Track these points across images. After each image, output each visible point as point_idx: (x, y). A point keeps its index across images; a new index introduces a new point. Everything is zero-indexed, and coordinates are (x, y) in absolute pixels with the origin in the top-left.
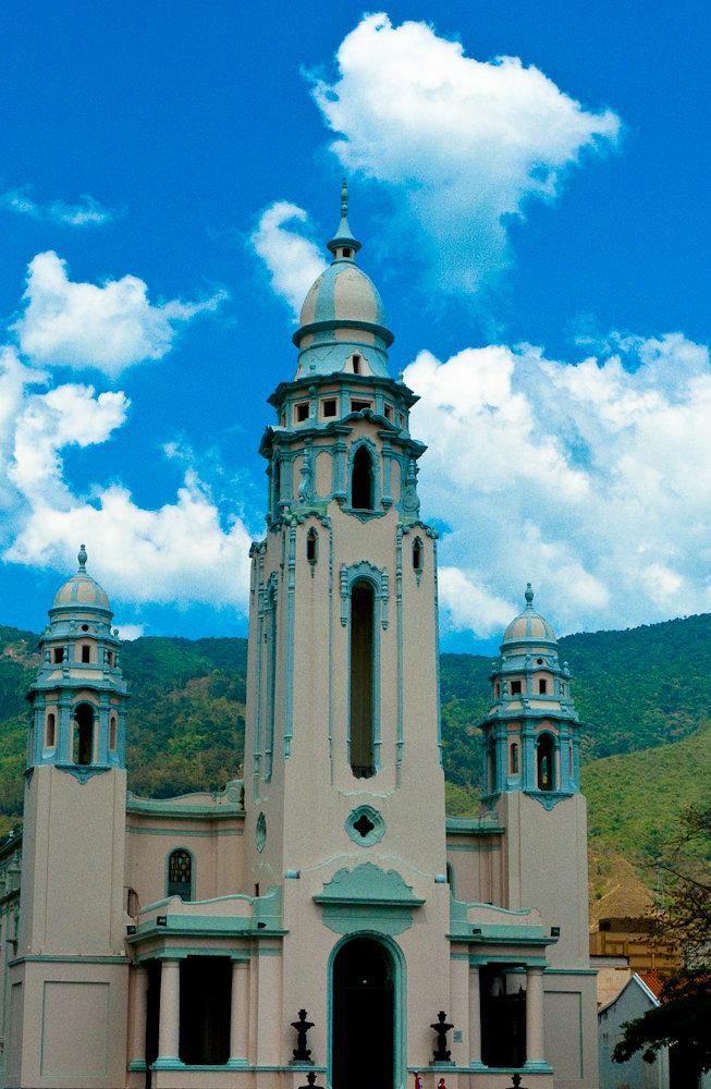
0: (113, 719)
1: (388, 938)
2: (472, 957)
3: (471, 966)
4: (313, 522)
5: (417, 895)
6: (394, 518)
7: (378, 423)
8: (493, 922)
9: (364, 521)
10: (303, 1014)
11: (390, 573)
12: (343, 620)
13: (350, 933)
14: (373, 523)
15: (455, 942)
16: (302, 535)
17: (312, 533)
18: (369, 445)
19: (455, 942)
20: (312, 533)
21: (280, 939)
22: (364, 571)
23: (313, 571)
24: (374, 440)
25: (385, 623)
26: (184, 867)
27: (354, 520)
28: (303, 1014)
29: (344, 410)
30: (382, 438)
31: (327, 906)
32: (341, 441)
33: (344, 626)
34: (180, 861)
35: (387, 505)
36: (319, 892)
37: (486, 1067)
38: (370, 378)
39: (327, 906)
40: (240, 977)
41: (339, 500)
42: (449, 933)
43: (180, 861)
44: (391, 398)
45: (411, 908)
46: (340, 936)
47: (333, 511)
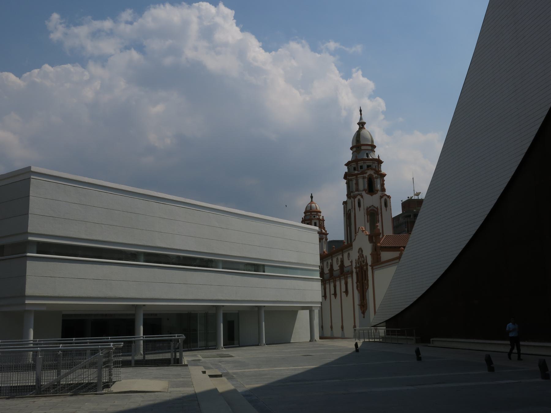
4: (359, 197)
7: (372, 169)
11: (379, 208)
14: (374, 196)
16: (356, 200)
17: (359, 200)
20: (359, 200)
25: (378, 221)
27: (369, 196)
29: (365, 167)
35: (378, 191)
47: (364, 193)
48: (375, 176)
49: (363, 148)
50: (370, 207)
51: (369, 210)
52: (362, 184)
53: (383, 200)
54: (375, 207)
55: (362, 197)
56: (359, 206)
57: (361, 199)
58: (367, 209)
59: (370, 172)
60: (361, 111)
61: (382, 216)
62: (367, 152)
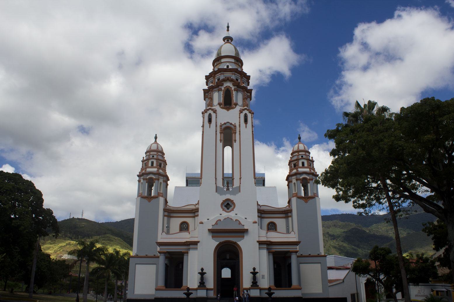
0: (161, 183)
1: (235, 243)
2: (268, 249)
3: (269, 252)
5: (246, 228)
6: (238, 108)
8: (274, 237)
9: (228, 110)
10: (202, 269)
12: (221, 140)
13: (221, 241)
14: (231, 111)
15: (261, 243)
17: (210, 115)
18: (230, 88)
19: (261, 243)
20: (210, 115)
21: (197, 244)
22: (228, 125)
23: (210, 126)
24: (231, 86)
25: (235, 141)
26: (185, 228)
27: (225, 111)
28: (202, 269)
30: (234, 85)
31: (214, 232)
32: (220, 87)
33: (221, 142)
34: (184, 226)
35: (236, 104)
36: (211, 228)
37: (276, 288)
38: (230, 69)
39: (214, 232)
40: (185, 257)
41: (220, 104)
42: (258, 240)
43: (184, 226)
44: (240, 76)
45: (242, 232)
46: (218, 243)
47: (218, 108)
48: (233, 89)
49: (223, 60)
50: (225, 124)
51: (224, 126)
52: (217, 97)
53: (242, 115)
54: (231, 124)
55: (215, 111)
56: (210, 121)
57: (214, 115)
58: (221, 126)
59: (229, 84)
60: (228, 27)
61: (240, 134)
62: (228, 64)
